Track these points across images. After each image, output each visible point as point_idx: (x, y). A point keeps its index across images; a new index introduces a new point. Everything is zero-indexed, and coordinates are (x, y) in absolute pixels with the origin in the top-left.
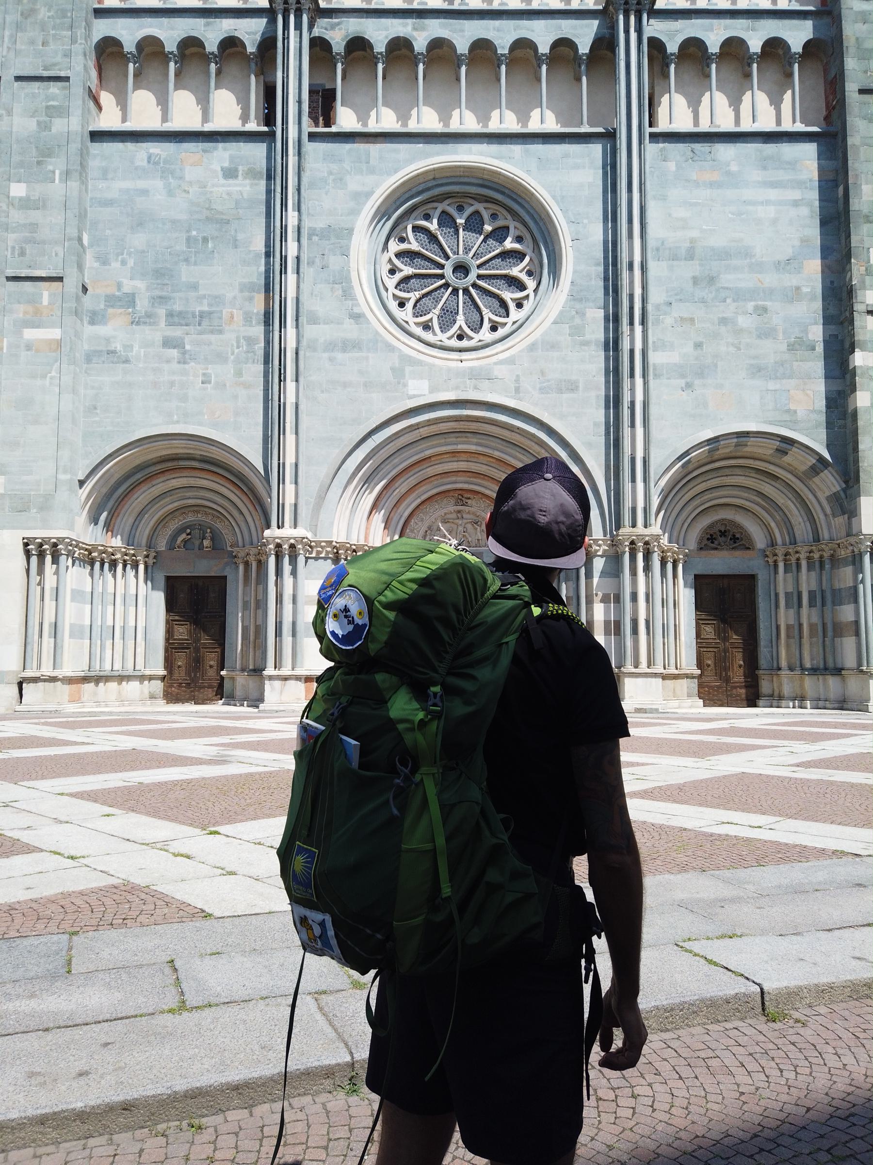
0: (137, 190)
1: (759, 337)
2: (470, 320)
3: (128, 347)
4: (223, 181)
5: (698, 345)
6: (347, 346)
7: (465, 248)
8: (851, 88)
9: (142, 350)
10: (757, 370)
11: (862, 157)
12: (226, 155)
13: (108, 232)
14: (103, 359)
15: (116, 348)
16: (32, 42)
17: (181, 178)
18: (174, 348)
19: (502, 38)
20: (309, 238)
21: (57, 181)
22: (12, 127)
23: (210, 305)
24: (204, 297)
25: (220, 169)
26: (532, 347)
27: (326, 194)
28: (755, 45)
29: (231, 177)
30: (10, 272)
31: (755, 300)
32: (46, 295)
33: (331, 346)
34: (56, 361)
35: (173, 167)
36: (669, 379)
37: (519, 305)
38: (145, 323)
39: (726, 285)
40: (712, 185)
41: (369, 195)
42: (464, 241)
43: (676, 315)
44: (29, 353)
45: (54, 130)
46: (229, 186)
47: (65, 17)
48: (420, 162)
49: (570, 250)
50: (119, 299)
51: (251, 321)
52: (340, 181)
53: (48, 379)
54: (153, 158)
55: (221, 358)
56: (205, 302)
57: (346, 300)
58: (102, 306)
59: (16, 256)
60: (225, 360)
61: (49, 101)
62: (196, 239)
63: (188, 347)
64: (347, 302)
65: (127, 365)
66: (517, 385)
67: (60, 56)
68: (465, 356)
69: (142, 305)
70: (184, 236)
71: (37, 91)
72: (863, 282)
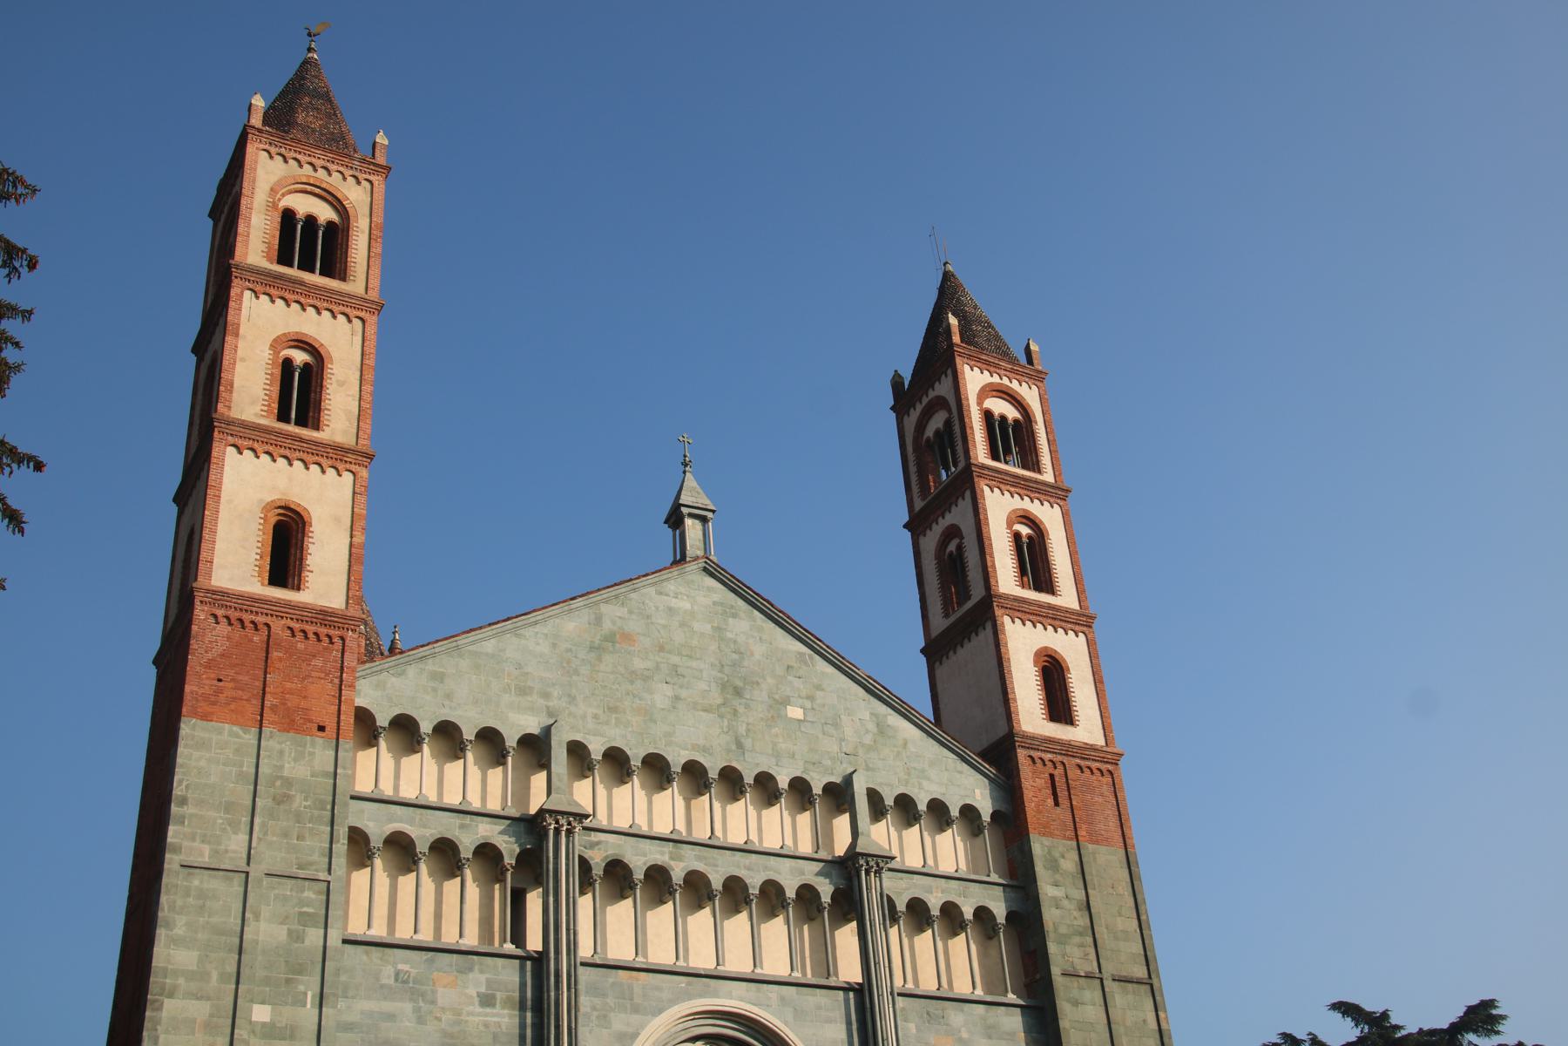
8: (1056, 971)
12: (483, 978)
16: (286, 835)
17: (433, 1002)
21: (309, 1006)
25: (475, 995)
27: (590, 1032)
28: (968, 912)
35: (424, 988)
41: (635, 1036)
45: (307, 942)
46: (486, 1015)
47: (325, 810)
52: (604, 1019)
61: (303, 906)
67: (317, 854)
71: (289, 893)
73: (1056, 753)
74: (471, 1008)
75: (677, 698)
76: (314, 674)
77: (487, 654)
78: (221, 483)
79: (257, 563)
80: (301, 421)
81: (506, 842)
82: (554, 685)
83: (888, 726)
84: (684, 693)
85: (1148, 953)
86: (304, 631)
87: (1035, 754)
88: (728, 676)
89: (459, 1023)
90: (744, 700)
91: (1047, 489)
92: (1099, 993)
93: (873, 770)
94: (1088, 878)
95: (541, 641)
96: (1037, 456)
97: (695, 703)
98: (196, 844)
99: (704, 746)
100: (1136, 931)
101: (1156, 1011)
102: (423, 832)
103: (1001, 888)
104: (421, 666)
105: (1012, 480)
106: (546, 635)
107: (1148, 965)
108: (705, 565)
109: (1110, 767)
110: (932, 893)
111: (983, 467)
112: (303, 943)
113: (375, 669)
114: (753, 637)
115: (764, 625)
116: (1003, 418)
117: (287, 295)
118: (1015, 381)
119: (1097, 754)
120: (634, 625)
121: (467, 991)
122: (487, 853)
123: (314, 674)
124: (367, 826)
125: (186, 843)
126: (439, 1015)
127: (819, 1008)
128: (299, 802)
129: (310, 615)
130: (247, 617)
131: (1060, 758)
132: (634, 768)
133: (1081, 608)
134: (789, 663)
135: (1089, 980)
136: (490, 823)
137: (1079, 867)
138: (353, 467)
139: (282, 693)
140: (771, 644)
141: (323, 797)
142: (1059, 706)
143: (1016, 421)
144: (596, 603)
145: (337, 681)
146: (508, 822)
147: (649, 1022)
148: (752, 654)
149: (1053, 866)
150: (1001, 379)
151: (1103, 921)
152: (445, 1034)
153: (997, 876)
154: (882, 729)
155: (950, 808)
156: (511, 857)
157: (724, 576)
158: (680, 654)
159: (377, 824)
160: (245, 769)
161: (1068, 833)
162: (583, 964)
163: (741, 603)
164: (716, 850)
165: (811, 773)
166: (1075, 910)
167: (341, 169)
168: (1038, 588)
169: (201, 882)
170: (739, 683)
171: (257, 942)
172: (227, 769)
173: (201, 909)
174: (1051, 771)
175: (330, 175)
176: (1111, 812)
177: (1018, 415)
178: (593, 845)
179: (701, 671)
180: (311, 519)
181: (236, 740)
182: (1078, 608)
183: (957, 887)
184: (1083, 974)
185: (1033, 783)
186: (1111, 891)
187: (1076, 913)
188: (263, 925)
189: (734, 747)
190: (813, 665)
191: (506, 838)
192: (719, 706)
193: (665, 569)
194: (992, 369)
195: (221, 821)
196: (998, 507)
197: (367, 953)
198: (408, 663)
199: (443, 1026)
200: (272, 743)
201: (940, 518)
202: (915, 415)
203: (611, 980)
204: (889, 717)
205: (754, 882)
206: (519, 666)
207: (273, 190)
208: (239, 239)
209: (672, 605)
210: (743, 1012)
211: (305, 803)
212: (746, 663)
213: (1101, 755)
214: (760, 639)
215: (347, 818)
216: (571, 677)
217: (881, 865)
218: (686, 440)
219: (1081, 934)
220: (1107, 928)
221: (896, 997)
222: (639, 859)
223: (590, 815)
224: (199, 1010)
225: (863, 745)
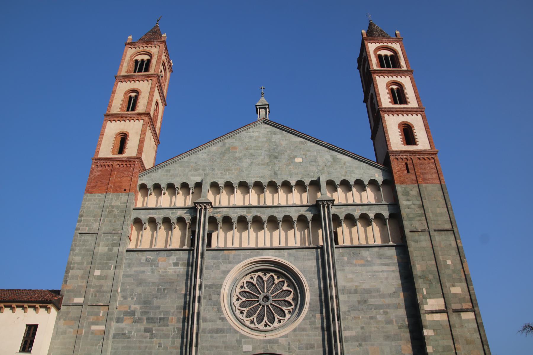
0: (140, 271)
2: (269, 319)
3: (130, 332)
4: (174, 267)
5: (362, 328)
6: (219, 331)
7: (267, 290)
8: (407, 231)
9: (136, 333)
10: (387, 337)
11: (415, 255)
12: (175, 258)
13: (128, 287)
14: (120, 337)
15: (126, 332)
16: (110, 221)
17: (158, 266)
18: (148, 332)
19: (279, 215)
20: (205, 288)
21: (112, 269)
22: (98, 251)
23: (164, 315)
24: (162, 311)
25: (172, 263)
26: (295, 330)
27: (212, 271)
28: (372, 215)
29: (176, 266)
30: (89, 303)
31: (383, 309)
32: (102, 312)
33: (211, 331)
34: (102, 339)
35: (155, 262)
36: (351, 342)
38: (138, 322)
39: (371, 303)
40: (361, 265)
41: (229, 271)
42: (266, 287)
43: (352, 316)
44: (92, 335)
45: (113, 251)
46: (175, 269)
47: (123, 213)
48: (248, 259)
49: (308, 291)
50: (129, 313)
51: (180, 321)
52: (218, 267)
53: (98, 346)
54: (148, 259)
55: (166, 336)
56: (162, 314)
57: (218, 312)
58: (122, 316)
59: (93, 297)
61: (114, 241)
62: (161, 289)
63: (154, 332)
64: (219, 313)
65: (129, 339)
66: (289, 346)
67: (119, 226)
68: (268, 334)
69: (138, 315)
70: (156, 288)
71: (109, 238)
72: (422, 302)
73: (408, 155)
74: (170, 267)
75: (252, 163)
76: (124, 176)
77: (185, 162)
78: (104, 131)
79: (112, 149)
81: (187, 216)
82: (207, 166)
83: (338, 158)
84: (254, 161)
85: (452, 219)
88: (272, 153)
89: (166, 272)
90: (278, 159)
91: (403, 72)
92: (428, 237)
93: (331, 174)
94: (422, 196)
96: (399, 63)
98: (84, 227)
99: (262, 176)
100: (446, 212)
101: (456, 239)
103: (387, 206)
105: (388, 72)
106: (206, 152)
107: (452, 224)
108: (263, 121)
109: (432, 156)
110: (356, 211)
112: (112, 251)
113: (148, 172)
114: (282, 139)
115: (287, 135)
116: (386, 56)
119: (426, 153)
120: (237, 144)
121: (169, 262)
122: (181, 220)
123: (124, 176)
124: (141, 217)
126: (159, 270)
127: (305, 255)
128: (116, 212)
129: (124, 160)
130: (106, 164)
131: (409, 157)
132: (235, 187)
133: (419, 106)
134: (297, 145)
135: (423, 232)
136: (182, 211)
137: (419, 193)
138: (143, 118)
139: (115, 182)
140: (289, 140)
141: (123, 209)
143: (391, 56)
144: (223, 140)
146: (188, 209)
147: (235, 266)
148: (282, 144)
149: (407, 194)
150: (384, 44)
151: (430, 210)
152: (161, 276)
153: (385, 202)
154: (335, 160)
155: (364, 182)
156: (188, 220)
157: (271, 123)
158: (254, 149)
159: (144, 216)
160: (101, 205)
161: (413, 182)
163: (278, 130)
164: (265, 208)
165: (304, 178)
166: (417, 208)
167: (151, 45)
168: (401, 103)
169: (85, 237)
170: (276, 154)
171: (98, 252)
172: (96, 206)
173: (83, 245)
174: (406, 162)
175: (148, 48)
177: (392, 53)
179: (262, 153)
180: (129, 134)
181: (100, 197)
182: (418, 106)
183: (367, 208)
184: (420, 230)
185: (397, 167)
186: (434, 199)
188: (100, 248)
189: (273, 175)
190: (306, 144)
191: (187, 214)
192: (268, 163)
195: (92, 220)
197: (137, 254)
198: (158, 169)
199: (160, 273)
202: (362, 66)
203: (221, 254)
204: (338, 155)
206: (196, 163)
207: (131, 56)
209: (252, 135)
210: (273, 260)
211: (118, 212)
212: (279, 148)
213: (429, 153)
214: (285, 139)
216: (213, 163)
217: (329, 203)
218: (262, 88)
219: (419, 216)
220: (432, 213)
222: (234, 215)
224: (80, 273)
225: (326, 166)
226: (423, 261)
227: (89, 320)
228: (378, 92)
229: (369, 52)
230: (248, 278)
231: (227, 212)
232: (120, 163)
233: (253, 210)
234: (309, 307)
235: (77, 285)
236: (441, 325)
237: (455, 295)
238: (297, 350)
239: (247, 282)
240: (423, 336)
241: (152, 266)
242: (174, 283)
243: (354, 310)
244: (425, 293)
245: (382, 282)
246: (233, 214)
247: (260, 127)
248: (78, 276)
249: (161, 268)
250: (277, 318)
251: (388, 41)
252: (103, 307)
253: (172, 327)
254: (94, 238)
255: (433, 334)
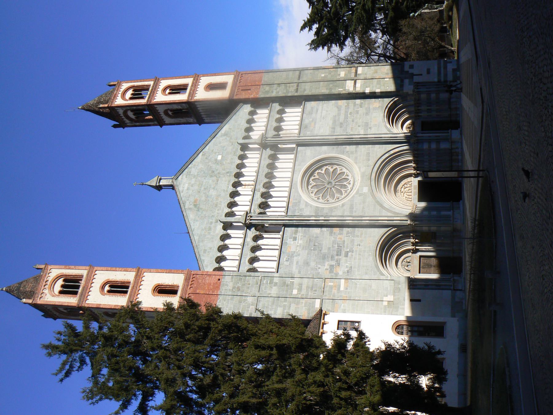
1: (358, 114)
3: (347, 267)
4: (297, 240)
5: (359, 126)
6: (352, 207)
8: (296, 94)
10: (367, 114)
12: (289, 240)
16: (248, 288)
17: (294, 252)
21: (294, 281)
23: (336, 244)
24: (333, 246)
26: (356, 163)
28: (278, 116)
29: (296, 238)
37: (341, 170)
40: (315, 124)
41: (306, 202)
46: (298, 239)
50: (331, 269)
52: (301, 210)
55: (353, 241)
56: (334, 245)
60: (353, 240)
63: (348, 250)
68: (356, 179)
69: (333, 263)
70: (313, 251)
75: (214, 188)
77: (199, 238)
78: (146, 307)
80: (127, 287)
82: (208, 221)
84: (212, 187)
86: (191, 285)
87: (235, 94)
89: (300, 245)
95: (196, 224)
97: (216, 184)
102: (248, 255)
104: (201, 256)
106: (194, 223)
110: (272, 125)
111: (148, 101)
112: (277, 283)
117: (88, 291)
118: (121, 90)
120: (192, 199)
125: (250, 312)
128: (239, 285)
142: (221, 86)
143: (133, 91)
144: (185, 209)
145: (206, 276)
149: (267, 92)
152: (303, 249)
154: (226, 134)
158: (201, 187)
159: (246, 266)
160: (230, 298)
162: (287, 214)
163: (186, 170)
167: (46, 277)
168: (186, 89)
172: (229, 302)
176: (253, 75)
178: (255, 212)
187: (281, 88)
189: (229, 174)
193: (175, 190)
194: (116, 96)
195: (244, 304)
196: (160, 97)
200: (223, 292)
201: (161, 116)
202: (127, 121)
203: (291, 208)
205: (266, 170)
206: (203, 230)
208: (69, 305)
215: (244, 273)
219: (286, 87)
221: (301, 135)
222: (259, 200)
223: (247, 212)
224: (293, 307)
226: (319, 88)
227: (336, 293)
228: (171, 101)
229: (126, 104)
230: (313, 195)
231: (255, 205)
232: (189, 287)
233: (257, 188)
234: (341, 154)
235: (304, 306)
236: (364, 83)
237: (345, 75)
238: (369, 162)
239: (315, 195)
240: (369, 94)
241: (294, 256)
242: (310, 239)
243: (346, 130)
244: (342, 89)
245: (329, 114)
246: (259, 201)
247: (179, 183)
248: (296, 307)
249: (297, 249)
250: (345, 176)
251: (117, 90)
252: (325, 282)
253: (346, 238)
254: (262, 299)
255: (369, 88)
